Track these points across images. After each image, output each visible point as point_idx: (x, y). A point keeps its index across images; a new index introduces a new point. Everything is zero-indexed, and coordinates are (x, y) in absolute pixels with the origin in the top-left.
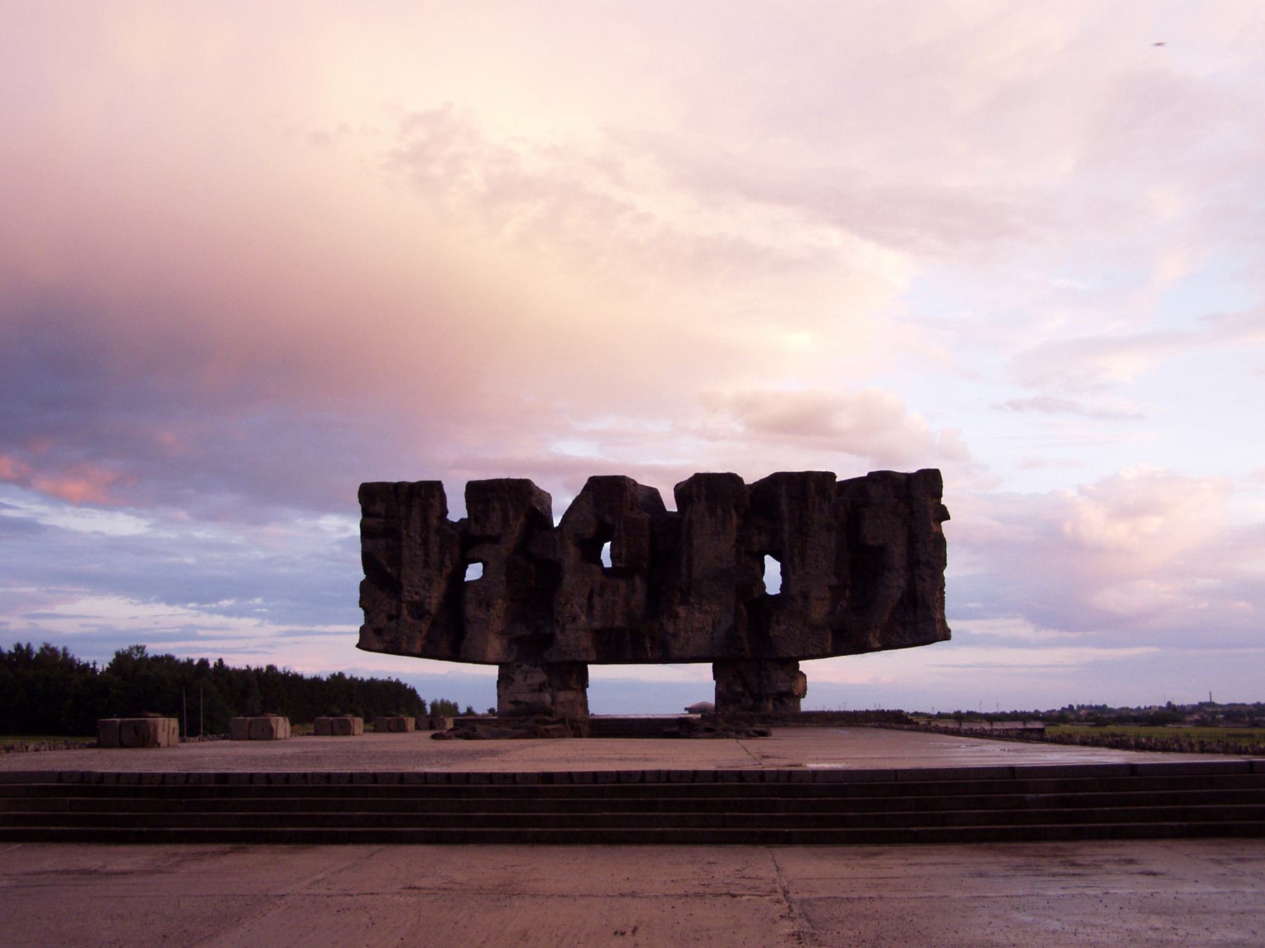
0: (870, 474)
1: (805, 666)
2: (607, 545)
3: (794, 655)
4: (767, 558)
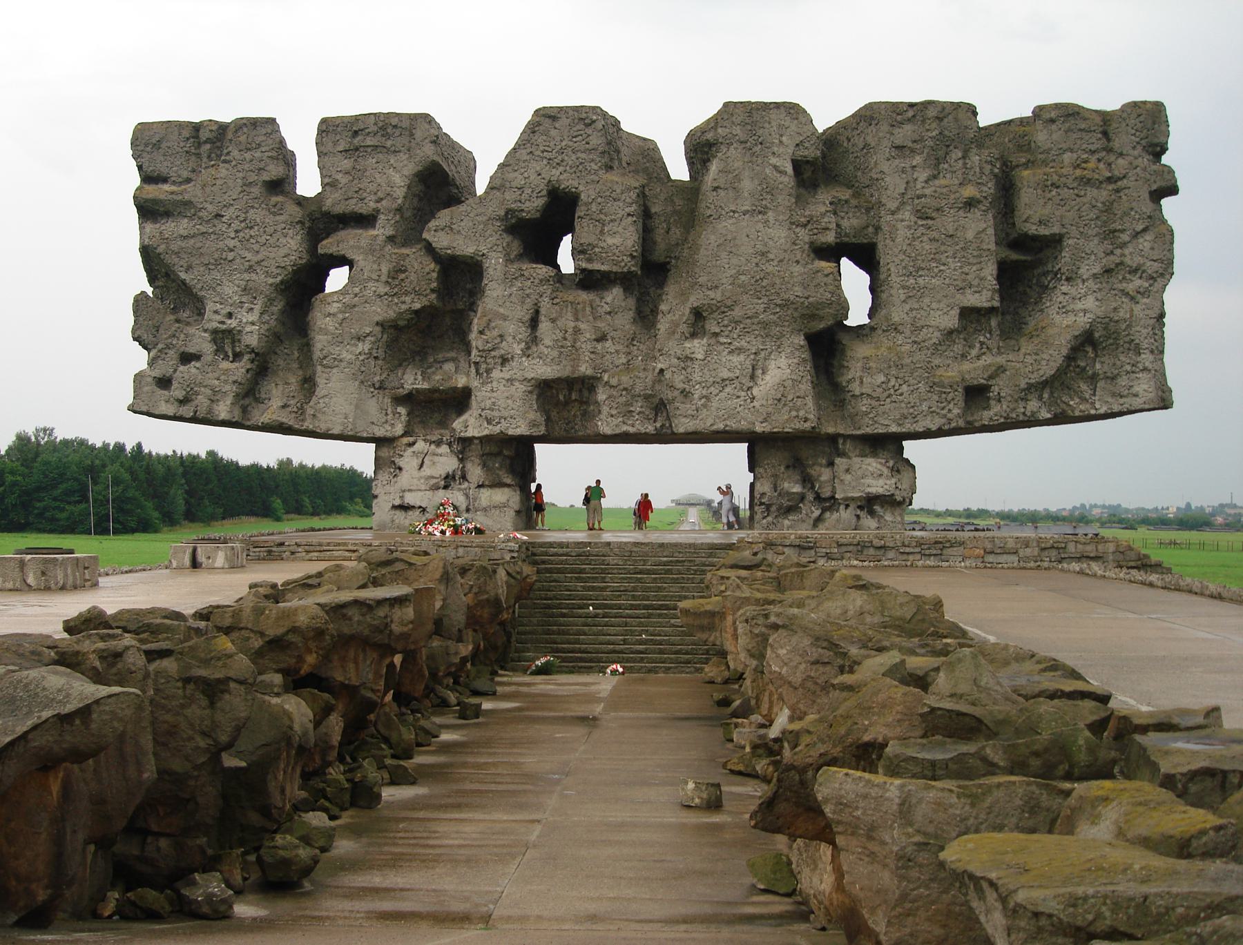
0: (1039, 111)
1: (911, 449)
3: (894, 429)
4: (845, 262)
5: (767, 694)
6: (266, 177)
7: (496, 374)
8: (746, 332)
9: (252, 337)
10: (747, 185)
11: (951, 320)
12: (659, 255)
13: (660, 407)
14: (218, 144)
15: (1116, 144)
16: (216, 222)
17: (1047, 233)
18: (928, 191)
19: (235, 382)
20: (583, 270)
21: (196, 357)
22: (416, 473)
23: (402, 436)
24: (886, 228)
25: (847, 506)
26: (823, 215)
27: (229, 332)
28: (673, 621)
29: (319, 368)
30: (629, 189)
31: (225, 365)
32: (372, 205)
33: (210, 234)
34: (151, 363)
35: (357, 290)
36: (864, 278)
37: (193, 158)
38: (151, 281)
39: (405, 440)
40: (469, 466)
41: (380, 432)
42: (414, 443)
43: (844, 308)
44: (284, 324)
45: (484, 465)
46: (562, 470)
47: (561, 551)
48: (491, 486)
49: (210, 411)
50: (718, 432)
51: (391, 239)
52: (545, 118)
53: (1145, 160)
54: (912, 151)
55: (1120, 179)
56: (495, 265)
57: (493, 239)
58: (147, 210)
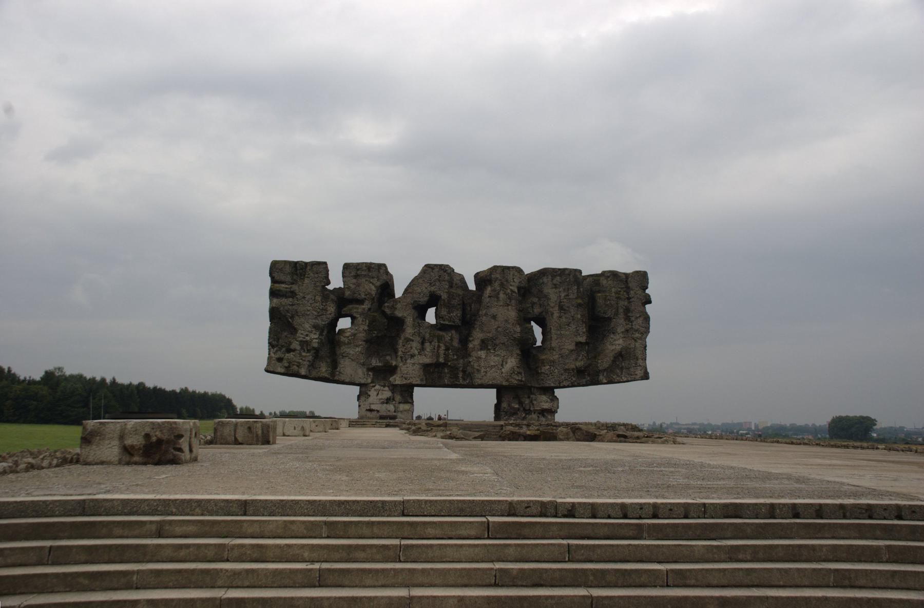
0: (604, 273)
1: (557, 392)
4: (533, 323)
7: (408, 361)
10: (502, 296)
11: (572, 347)
21: (294, 350)
31: (304, 354)
36: (540, 330)
41: (363, 381)
45: (401, 395)
52: (428, 268)
53: (640, 292)
56: (409, 321)
58: (273, 293)
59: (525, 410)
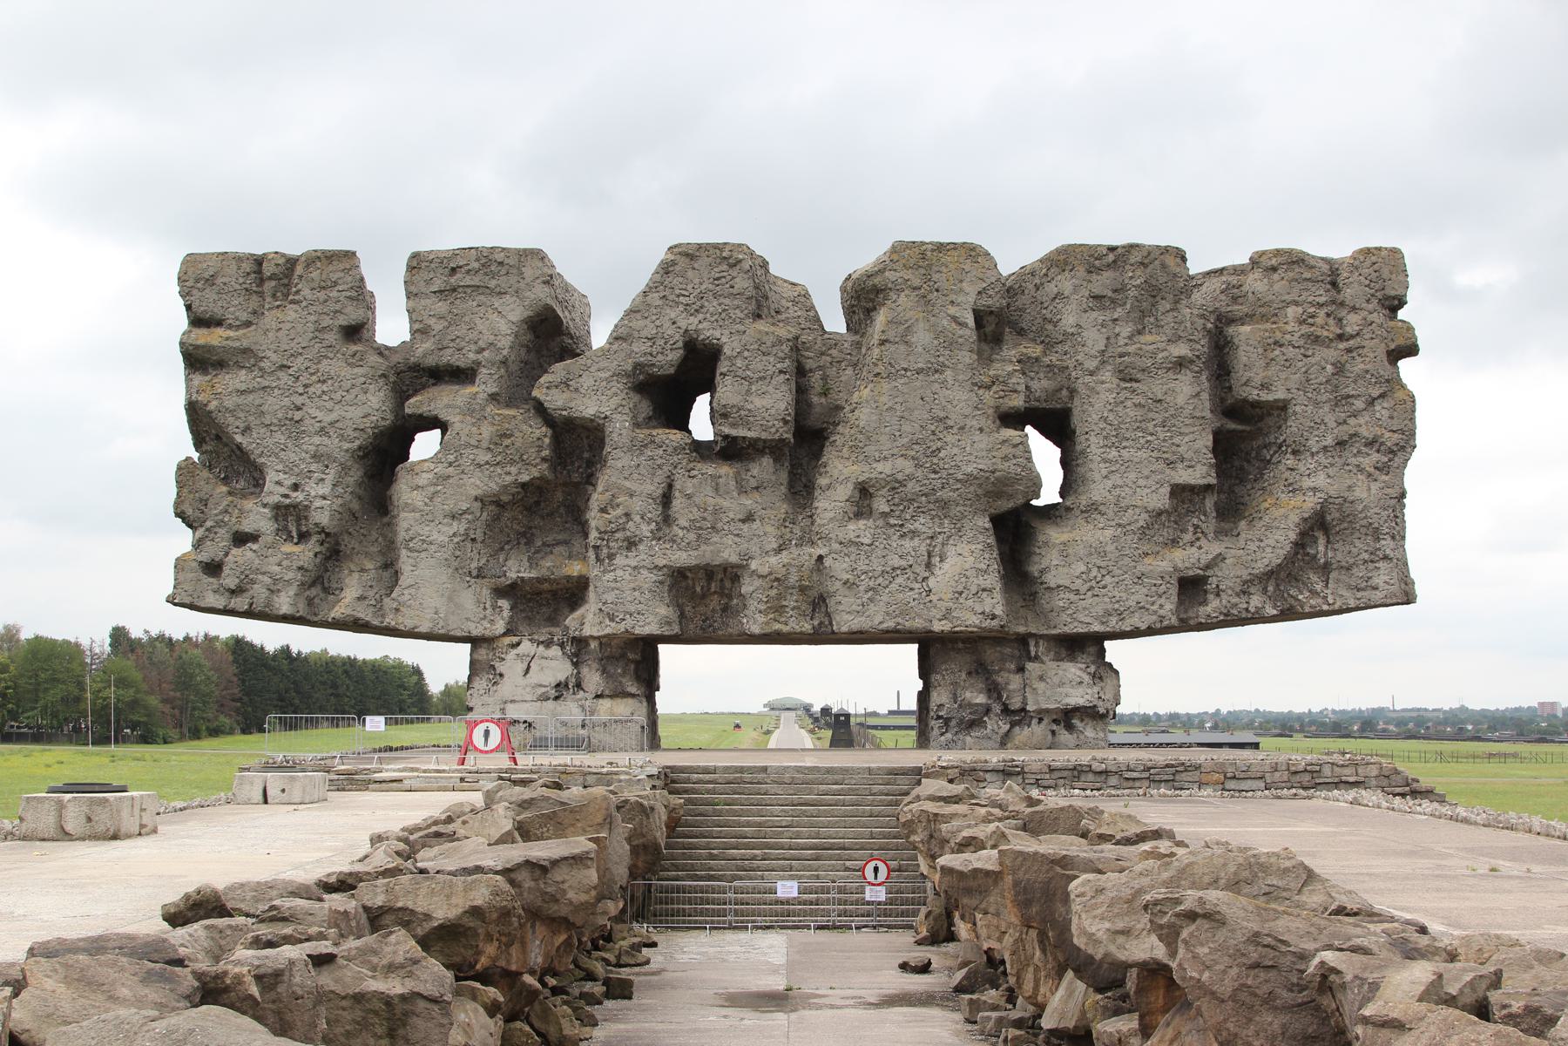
2: (702, 404)
3: (1097, 627)
4: (1029, 429)
5: (1031, 969)
6: (343, 321)
8: (920, 511)
9: (322, 516)
11: (1160, 499)
12: (813, 422)
13: (819, 603)
14: (285, 281)
15: (1348, 294)
16: (281, 374)
17: (1270, 398)
18: (1131, 349)
19: (300, 568)
20: (726, 437)
21: (253, 537)
22: (521, 681)
23: (504, 635)
24: (1082, 390)
25: (1041, 720)
26: (1010, 375)
27: (295, 506)
28: (848, 863)
29: (404, 552)
30: (780, 341)
31: (288, 548)
32: (472, 356)
33: (273, 389)
34: (198, 545)
35: (451, 458)
36: (1056, 452)
37: (254, 297)
38: (198, 445)
39: (508, 640)
40: (585, 670)
41: (476, 631)
42: (518, 644)
43: (1035, 486)
44: (360, 498)
45: (604, 672)
46: (695, 678)
47: (708, 777)
48: (611, 697)
49: (268, 604)
50: (888, 632)
51: (493, 397)
52: (684, 258)
54: (1113, 301)
55: (1352, 337)
56: (620, 429)
57: (615, 401)
58: (196, 360)
59: (1006, 710)
